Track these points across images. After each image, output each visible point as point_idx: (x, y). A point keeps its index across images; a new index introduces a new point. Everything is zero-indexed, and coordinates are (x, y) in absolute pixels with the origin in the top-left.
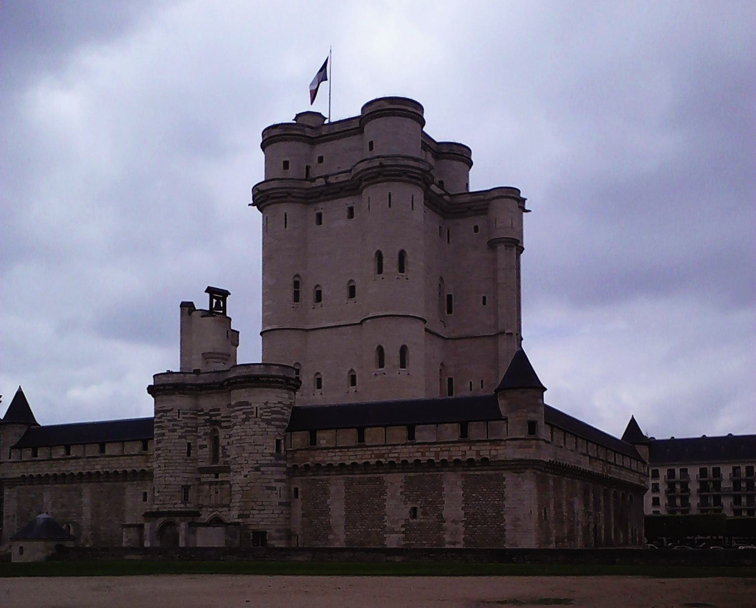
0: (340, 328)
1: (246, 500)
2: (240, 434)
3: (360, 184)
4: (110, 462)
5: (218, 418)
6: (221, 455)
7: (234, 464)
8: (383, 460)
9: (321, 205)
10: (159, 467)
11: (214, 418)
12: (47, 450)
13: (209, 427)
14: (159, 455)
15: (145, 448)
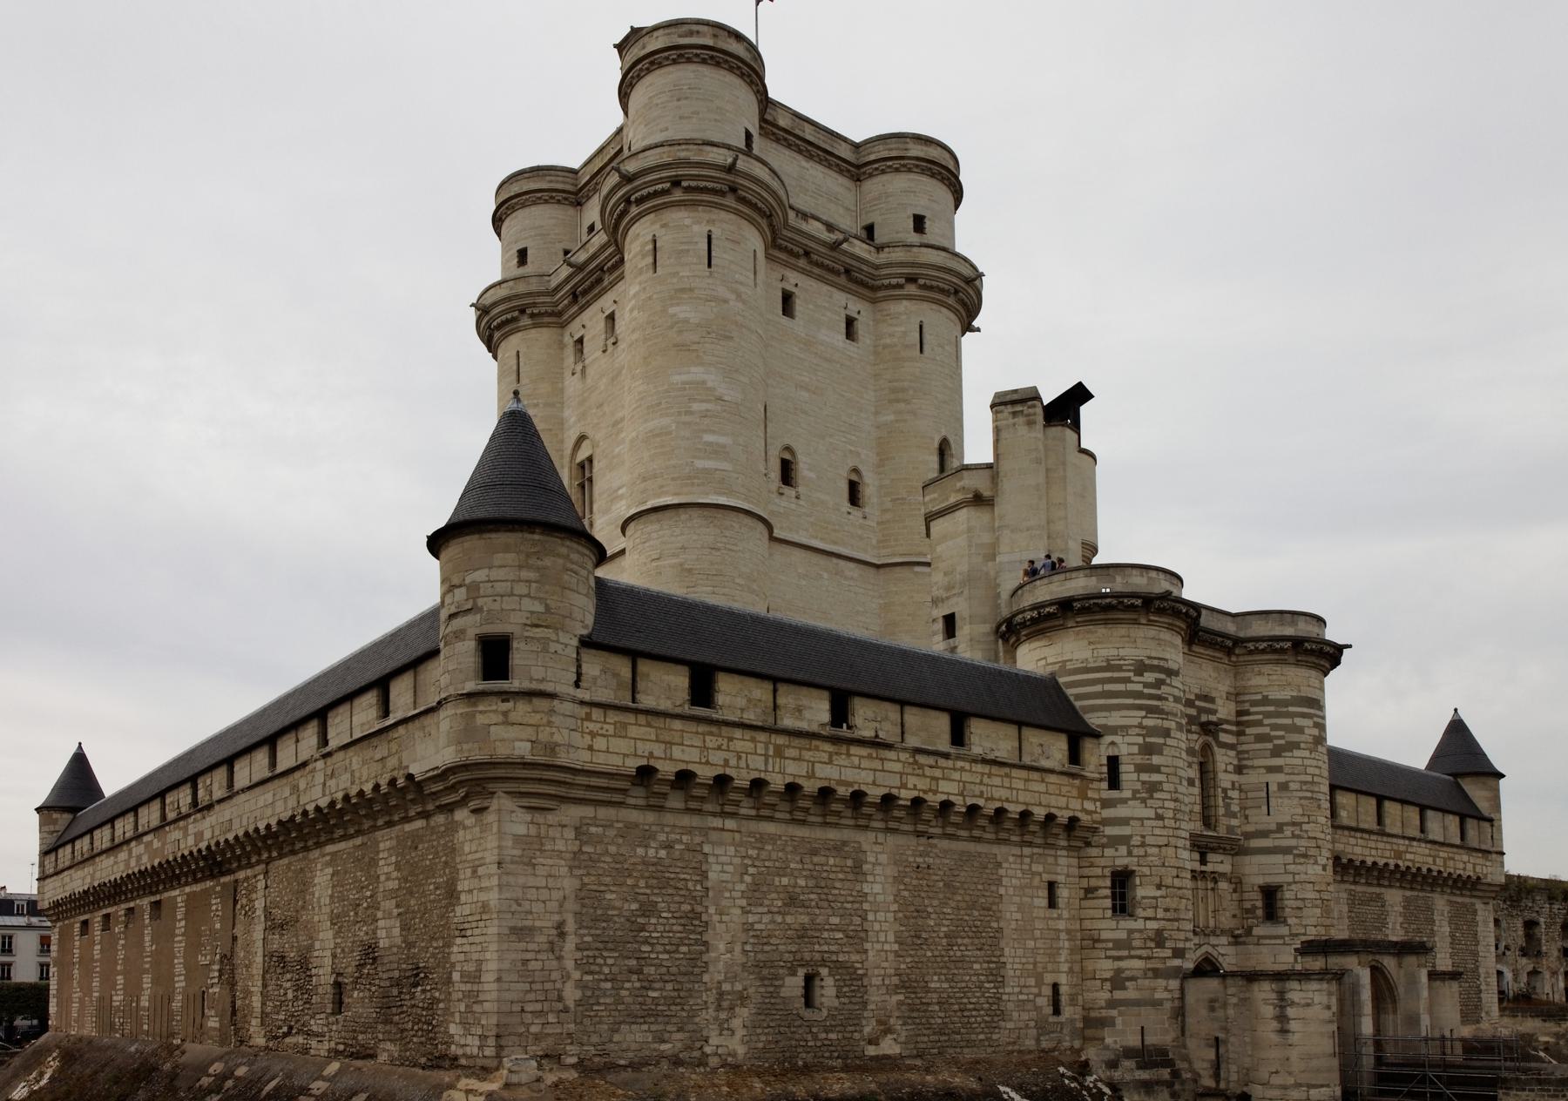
0: (835, 560)
1: (1328, 922)
2: (1310, 770)
3: (900, 286)
4: (986, 780)
5: (1213, 718)
6: (1221, 811)
7: (1294, 836)
8: (1400, 863)
9: (793, 277)
10: (1159, 817)
11: (1204, 718)
12: (760, 692)
13: (1195, 737)
14: (1153, 788)
15: (1075, 756)
